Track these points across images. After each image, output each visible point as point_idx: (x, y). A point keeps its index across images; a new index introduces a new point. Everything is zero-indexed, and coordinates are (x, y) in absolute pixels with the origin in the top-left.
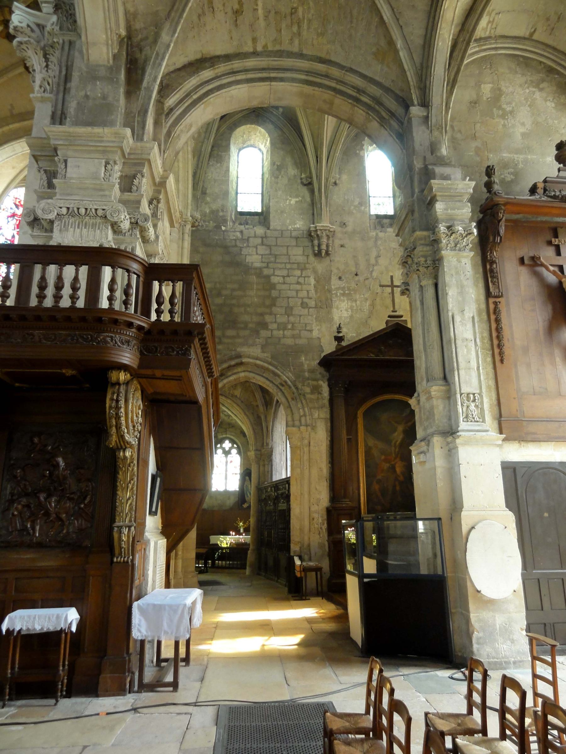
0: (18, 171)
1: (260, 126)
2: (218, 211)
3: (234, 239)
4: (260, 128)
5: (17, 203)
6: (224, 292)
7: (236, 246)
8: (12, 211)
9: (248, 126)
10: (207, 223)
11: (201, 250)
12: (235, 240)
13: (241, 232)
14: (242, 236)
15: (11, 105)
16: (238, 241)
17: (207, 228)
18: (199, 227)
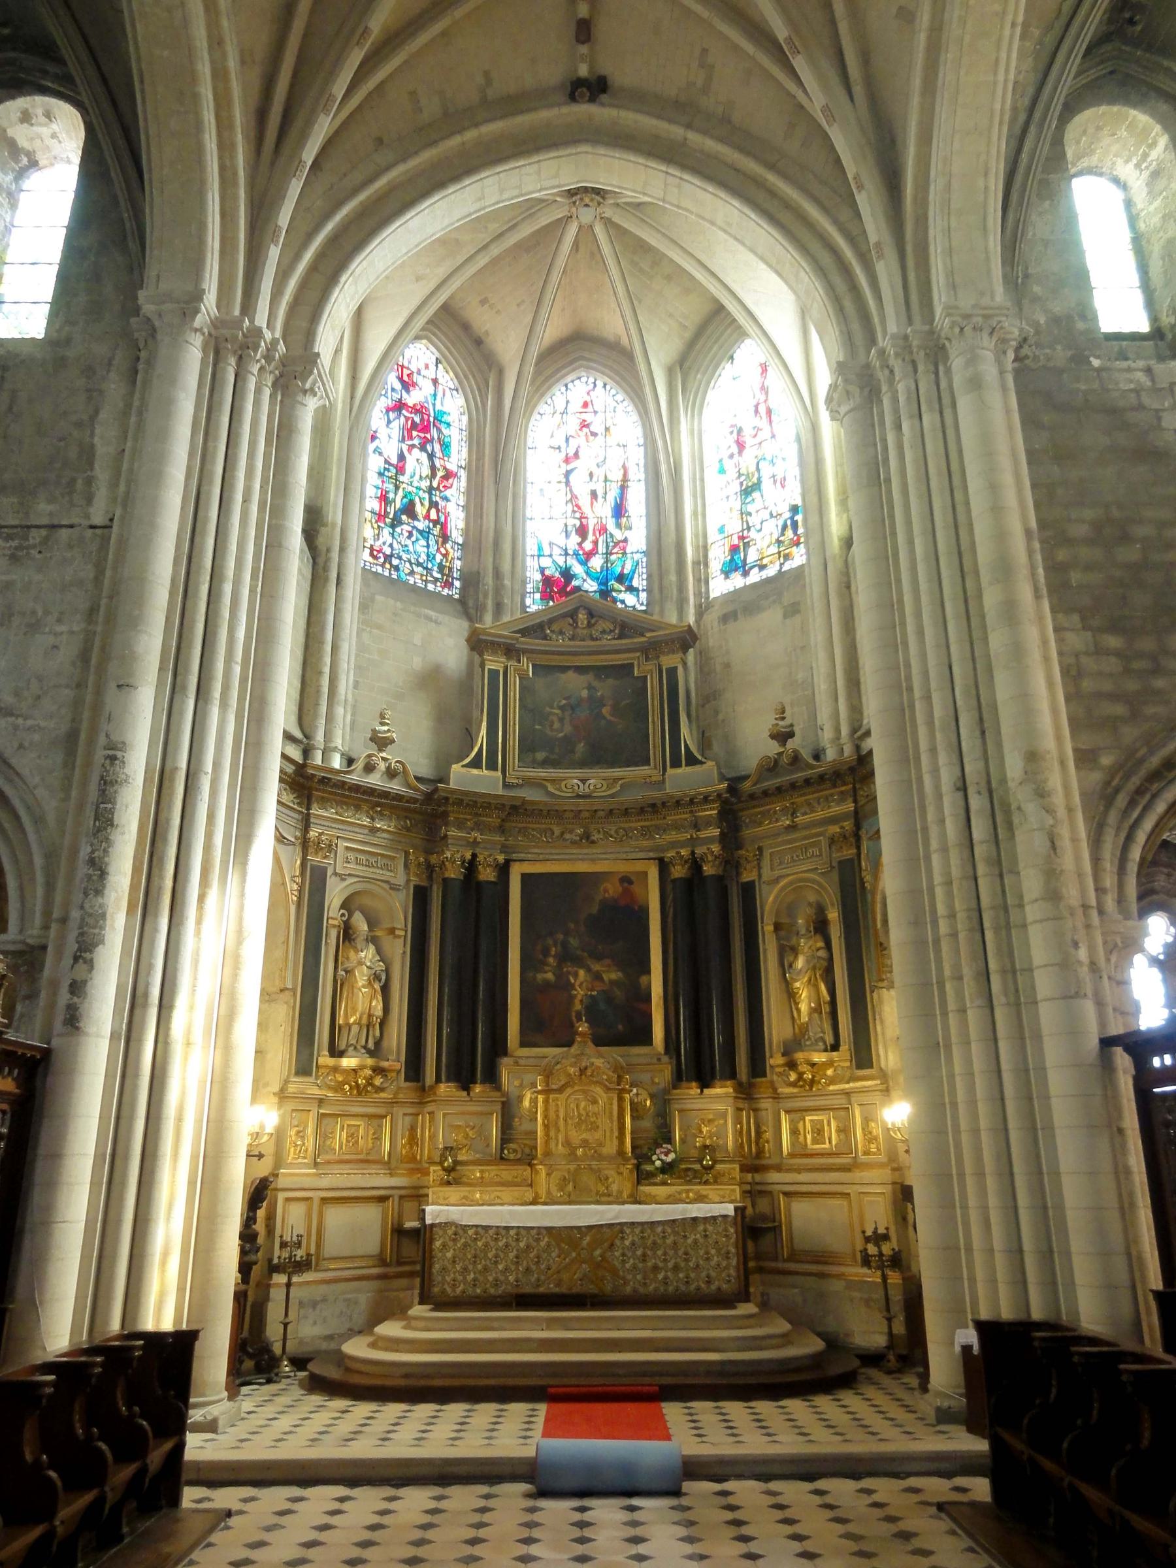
0: (432, 285)
1: (1134, 106)
2: (1069, 318)
3: (1131, 390)
4: (1133, 113)
5: (406, 378)
6: (1141, 531)
7: (1141, 407)
8: (396, 396)
9: (1103, 109)
10: (1048, 351)
11: (1046, 419)
12: (1137, 392)
13: (1148, 371)
14: (1153, 381)
15: (487, 74)
16: (1143, 394)
17: (1051, 364)
18: (1027, 362)
